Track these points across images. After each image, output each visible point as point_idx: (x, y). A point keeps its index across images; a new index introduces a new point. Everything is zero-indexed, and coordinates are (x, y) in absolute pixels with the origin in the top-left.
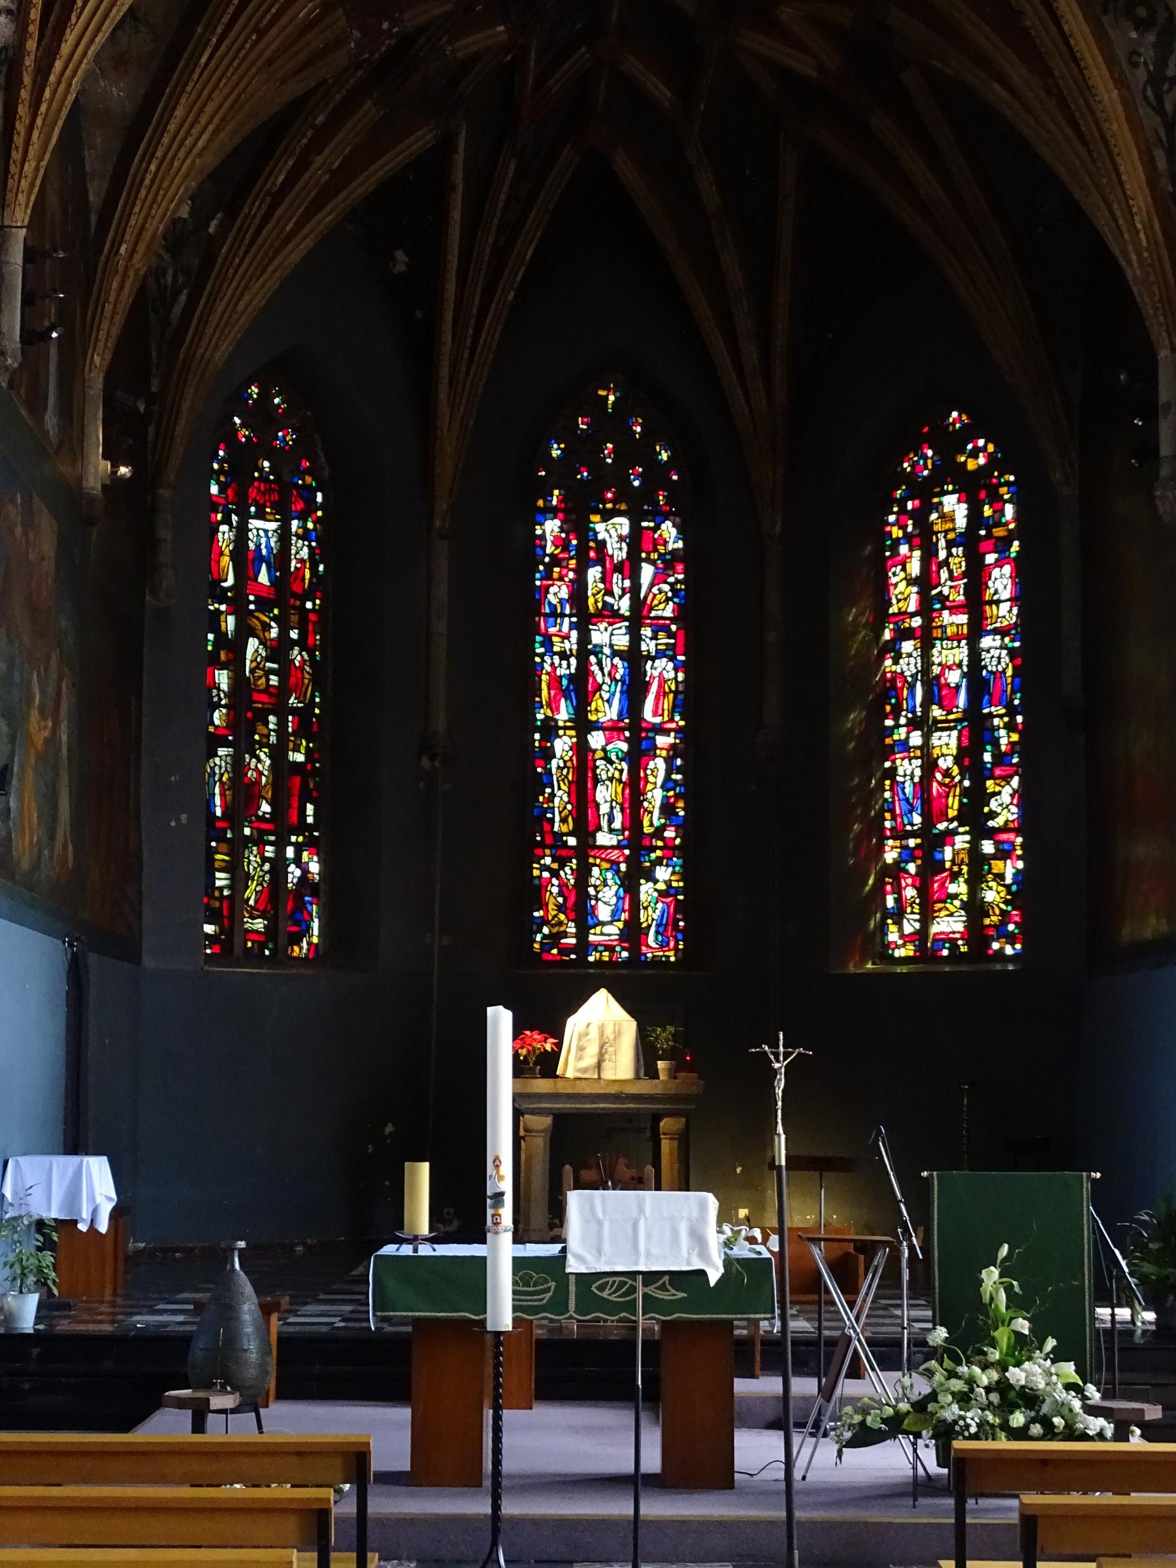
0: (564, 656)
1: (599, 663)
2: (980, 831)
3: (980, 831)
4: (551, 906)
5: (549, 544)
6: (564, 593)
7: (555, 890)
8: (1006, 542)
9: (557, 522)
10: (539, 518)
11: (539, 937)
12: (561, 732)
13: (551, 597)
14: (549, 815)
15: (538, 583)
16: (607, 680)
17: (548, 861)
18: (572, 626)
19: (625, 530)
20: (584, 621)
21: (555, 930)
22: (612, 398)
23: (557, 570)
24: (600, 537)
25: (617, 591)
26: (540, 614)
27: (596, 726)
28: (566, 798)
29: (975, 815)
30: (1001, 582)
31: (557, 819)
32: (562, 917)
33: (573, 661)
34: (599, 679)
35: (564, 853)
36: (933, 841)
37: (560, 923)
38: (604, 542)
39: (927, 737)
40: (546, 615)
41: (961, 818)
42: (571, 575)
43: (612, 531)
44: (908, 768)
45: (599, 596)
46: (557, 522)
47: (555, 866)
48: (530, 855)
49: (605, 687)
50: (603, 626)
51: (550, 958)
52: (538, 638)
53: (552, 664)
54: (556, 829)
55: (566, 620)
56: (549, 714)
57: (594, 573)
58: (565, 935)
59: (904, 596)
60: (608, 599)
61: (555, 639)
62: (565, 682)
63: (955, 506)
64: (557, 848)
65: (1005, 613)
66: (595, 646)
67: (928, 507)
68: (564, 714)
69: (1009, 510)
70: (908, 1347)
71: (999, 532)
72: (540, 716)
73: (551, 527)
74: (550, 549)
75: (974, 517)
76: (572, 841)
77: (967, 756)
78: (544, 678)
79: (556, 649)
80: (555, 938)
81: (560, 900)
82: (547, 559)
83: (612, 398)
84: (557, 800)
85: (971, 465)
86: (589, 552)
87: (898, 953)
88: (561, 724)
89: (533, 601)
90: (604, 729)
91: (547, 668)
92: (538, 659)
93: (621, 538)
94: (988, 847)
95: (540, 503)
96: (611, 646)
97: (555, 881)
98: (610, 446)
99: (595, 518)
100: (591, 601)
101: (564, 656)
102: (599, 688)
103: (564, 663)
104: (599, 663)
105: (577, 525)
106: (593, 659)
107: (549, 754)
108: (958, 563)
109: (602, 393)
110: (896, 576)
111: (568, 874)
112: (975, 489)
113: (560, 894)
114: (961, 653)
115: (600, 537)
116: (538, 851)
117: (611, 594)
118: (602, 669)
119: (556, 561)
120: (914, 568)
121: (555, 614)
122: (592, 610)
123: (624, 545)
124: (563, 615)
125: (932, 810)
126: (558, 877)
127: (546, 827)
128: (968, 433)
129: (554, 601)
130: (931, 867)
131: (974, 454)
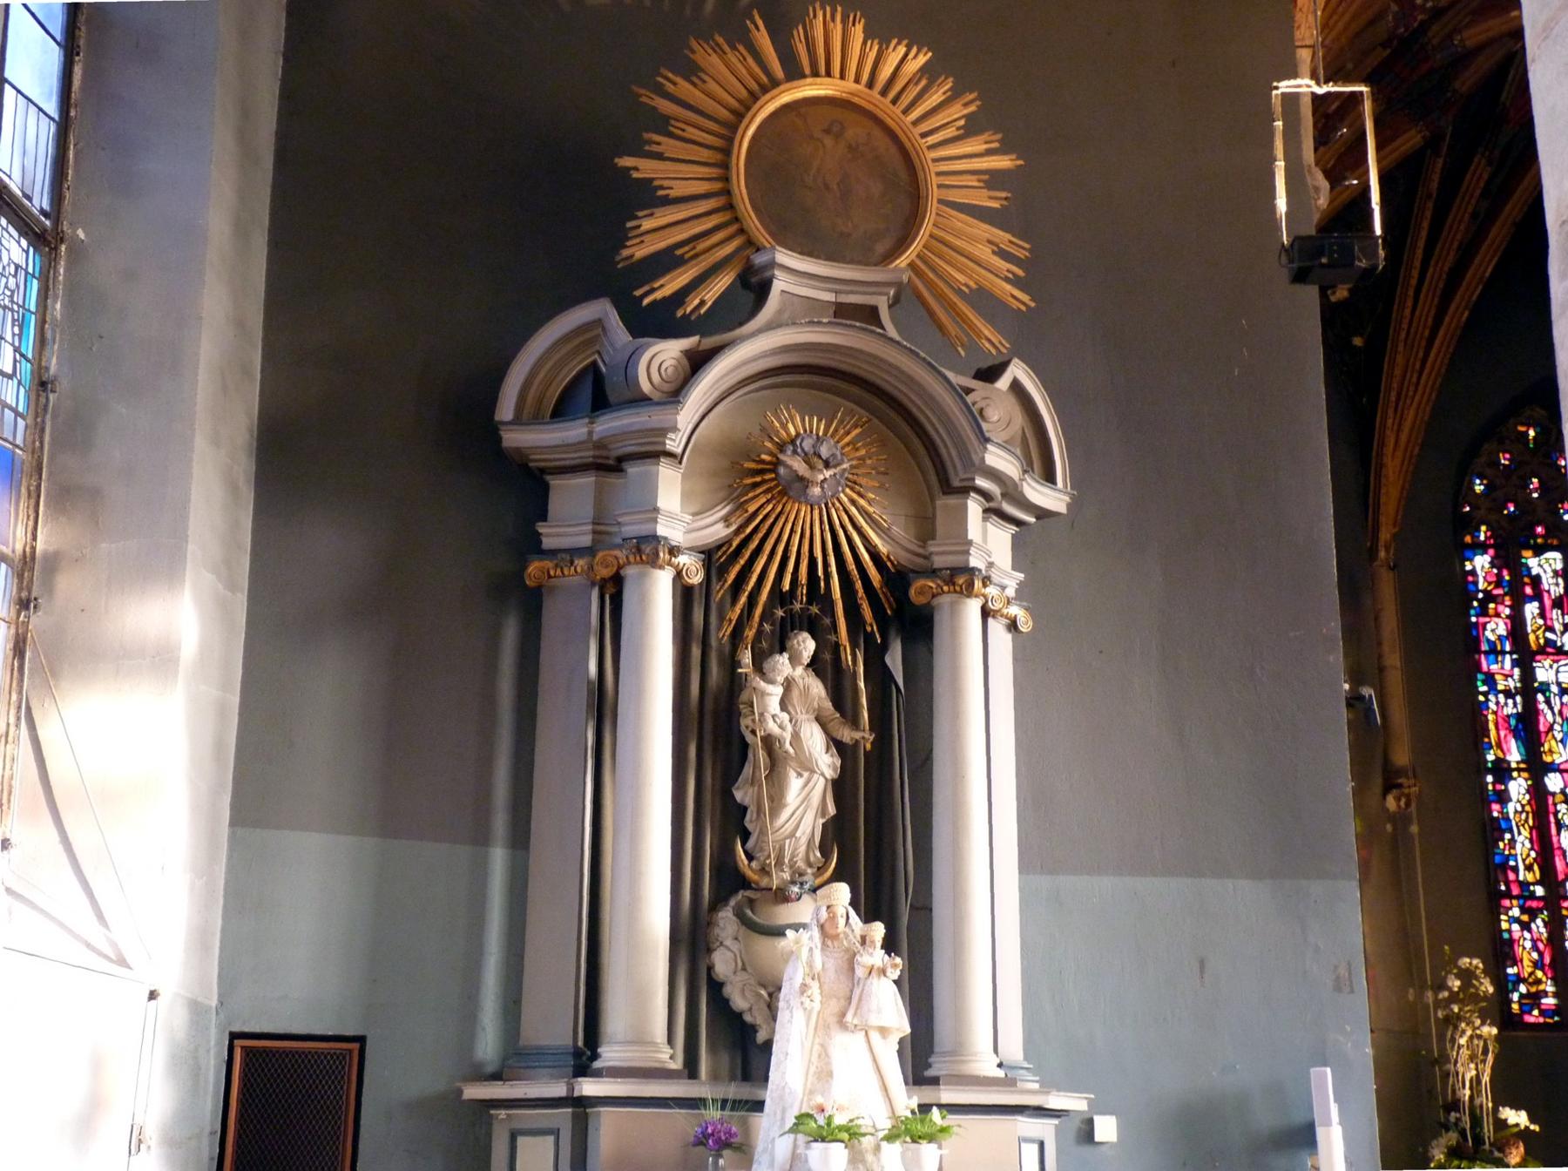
0: (1508, 694)
1: (1548, 702)
4: (1526, 962)
5: (1481, 580)
6: (1502, 630)
7: (1528, 944)
9: (1487, 558)
10: (1468, 554)
11: (1515, 997)
12: (1515, 774)
13: (1488, 634)
14: (1512, 863)
15: (1474, 619)
16: (1559, 719)
17: (1516, 912)
18: (1515, 663)
19: (1559, 566)
20: (1526, 658)
21: (1533, 989)
22: (1532, 433)
23: (1492, 606)
24: (1534, 572)
25: (1558, 627)
26: (1480, 652)
27: (1552, 768)
28: (1528, 845)
31: (1521, 867)
32: (1539, 974)
33: (1518, 699)
34: (1550, 718)
35: (1534, 904)
37: (1539, 982)
38: (1538, 577)
40: (1486, 653)
42: (1507, 611)
43: (1546, 566)
45: (1540, 632)
46: (1487, 558)
47: (1525, 918)
48: (1495, 911)
49: (1557, 727)
50: (1547, 663)
51: (1532, 1020)
52: (1480, 676)
53: (1497, 703)
54: (1521, 878)
55: (1508, 657)
56: (1500, 755)
57: (1531, 609)
58: (1545, 994)
60: (1549, 635)
61: (1498, 677)
62: (1513, 722)
64: (1526, 899)
66: (1541, 683)
68: (1514, 755)
72: (1490, 757)
73: (1481, 562)
74: (1482, 585)
76: (1540, 891)
78: (1491, 717)
79: (1500, 687)
80: (1534, 998)
81: (1535, 955)
82: (1481, 595)
83: (1532, 433)
84: (1518, 846)
86: (1520, 587)
88: (1514, 765)
89: (1471, 640)
90: (1561, 771)
91: (1492, 706)
92: (1481, 698)
93: (1556, 573)
95: (1468, 539)
96: (1559, 684)
97: (1527, 935)
98: (1535, 480)
99: (1527, 553)
100: (1532, 638)
101: (1508, 694)
102: (1551, 728)
103: (1510, 701)
104: (1548, 702)
105: (1508, 558)
106: (1540, 697)
107: (1503, 798)
109: (1522, 429)
111: (1539, 926)
113: (1535, 948)
115: (1534, 572)
116: (1507, 903)
117: (1551, 629)
118: (1551, 708)
119: (1489, 598)
121: (1495, 652)
122: (1534, 646)
123: (1560, 581)
124: (1503, 653)
126: (1530, 931)
127: (1511, 876)
129: (1492, 638)
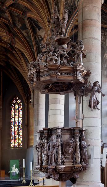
2: (19, 136)
3: (19, 136)
8: (21, 109)
29: (18, 134)
30: (21, 113)
36: (15, 137)
39: (15, 127)
41: (17, 135)
44: (13, 130)
59: (13, 114)
63: (17, 106)
65: (21, 116)
67: (15, 106)
69: (22, 106)
70: (10, 180)
71: (21, 108)
75: (19, 107)
77: (18, 129)
85: (19, 102)
87: (12, 147)
94: (19, 137)
108: (17, 111)
110: (12, 112)
112: (19, 104)
114: (17, 119)
120: (14, 112)
125: (15, 134)
128: (18, 99)
130: (15, 139)
131: (19, 101)
